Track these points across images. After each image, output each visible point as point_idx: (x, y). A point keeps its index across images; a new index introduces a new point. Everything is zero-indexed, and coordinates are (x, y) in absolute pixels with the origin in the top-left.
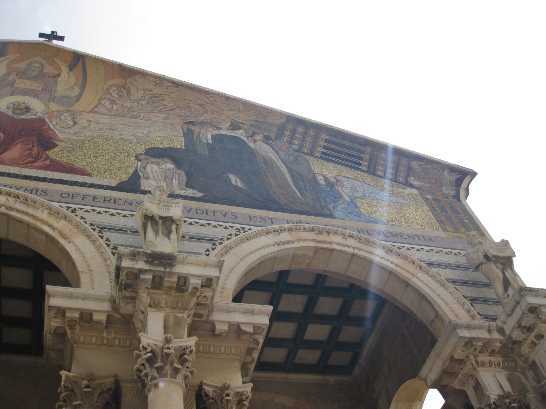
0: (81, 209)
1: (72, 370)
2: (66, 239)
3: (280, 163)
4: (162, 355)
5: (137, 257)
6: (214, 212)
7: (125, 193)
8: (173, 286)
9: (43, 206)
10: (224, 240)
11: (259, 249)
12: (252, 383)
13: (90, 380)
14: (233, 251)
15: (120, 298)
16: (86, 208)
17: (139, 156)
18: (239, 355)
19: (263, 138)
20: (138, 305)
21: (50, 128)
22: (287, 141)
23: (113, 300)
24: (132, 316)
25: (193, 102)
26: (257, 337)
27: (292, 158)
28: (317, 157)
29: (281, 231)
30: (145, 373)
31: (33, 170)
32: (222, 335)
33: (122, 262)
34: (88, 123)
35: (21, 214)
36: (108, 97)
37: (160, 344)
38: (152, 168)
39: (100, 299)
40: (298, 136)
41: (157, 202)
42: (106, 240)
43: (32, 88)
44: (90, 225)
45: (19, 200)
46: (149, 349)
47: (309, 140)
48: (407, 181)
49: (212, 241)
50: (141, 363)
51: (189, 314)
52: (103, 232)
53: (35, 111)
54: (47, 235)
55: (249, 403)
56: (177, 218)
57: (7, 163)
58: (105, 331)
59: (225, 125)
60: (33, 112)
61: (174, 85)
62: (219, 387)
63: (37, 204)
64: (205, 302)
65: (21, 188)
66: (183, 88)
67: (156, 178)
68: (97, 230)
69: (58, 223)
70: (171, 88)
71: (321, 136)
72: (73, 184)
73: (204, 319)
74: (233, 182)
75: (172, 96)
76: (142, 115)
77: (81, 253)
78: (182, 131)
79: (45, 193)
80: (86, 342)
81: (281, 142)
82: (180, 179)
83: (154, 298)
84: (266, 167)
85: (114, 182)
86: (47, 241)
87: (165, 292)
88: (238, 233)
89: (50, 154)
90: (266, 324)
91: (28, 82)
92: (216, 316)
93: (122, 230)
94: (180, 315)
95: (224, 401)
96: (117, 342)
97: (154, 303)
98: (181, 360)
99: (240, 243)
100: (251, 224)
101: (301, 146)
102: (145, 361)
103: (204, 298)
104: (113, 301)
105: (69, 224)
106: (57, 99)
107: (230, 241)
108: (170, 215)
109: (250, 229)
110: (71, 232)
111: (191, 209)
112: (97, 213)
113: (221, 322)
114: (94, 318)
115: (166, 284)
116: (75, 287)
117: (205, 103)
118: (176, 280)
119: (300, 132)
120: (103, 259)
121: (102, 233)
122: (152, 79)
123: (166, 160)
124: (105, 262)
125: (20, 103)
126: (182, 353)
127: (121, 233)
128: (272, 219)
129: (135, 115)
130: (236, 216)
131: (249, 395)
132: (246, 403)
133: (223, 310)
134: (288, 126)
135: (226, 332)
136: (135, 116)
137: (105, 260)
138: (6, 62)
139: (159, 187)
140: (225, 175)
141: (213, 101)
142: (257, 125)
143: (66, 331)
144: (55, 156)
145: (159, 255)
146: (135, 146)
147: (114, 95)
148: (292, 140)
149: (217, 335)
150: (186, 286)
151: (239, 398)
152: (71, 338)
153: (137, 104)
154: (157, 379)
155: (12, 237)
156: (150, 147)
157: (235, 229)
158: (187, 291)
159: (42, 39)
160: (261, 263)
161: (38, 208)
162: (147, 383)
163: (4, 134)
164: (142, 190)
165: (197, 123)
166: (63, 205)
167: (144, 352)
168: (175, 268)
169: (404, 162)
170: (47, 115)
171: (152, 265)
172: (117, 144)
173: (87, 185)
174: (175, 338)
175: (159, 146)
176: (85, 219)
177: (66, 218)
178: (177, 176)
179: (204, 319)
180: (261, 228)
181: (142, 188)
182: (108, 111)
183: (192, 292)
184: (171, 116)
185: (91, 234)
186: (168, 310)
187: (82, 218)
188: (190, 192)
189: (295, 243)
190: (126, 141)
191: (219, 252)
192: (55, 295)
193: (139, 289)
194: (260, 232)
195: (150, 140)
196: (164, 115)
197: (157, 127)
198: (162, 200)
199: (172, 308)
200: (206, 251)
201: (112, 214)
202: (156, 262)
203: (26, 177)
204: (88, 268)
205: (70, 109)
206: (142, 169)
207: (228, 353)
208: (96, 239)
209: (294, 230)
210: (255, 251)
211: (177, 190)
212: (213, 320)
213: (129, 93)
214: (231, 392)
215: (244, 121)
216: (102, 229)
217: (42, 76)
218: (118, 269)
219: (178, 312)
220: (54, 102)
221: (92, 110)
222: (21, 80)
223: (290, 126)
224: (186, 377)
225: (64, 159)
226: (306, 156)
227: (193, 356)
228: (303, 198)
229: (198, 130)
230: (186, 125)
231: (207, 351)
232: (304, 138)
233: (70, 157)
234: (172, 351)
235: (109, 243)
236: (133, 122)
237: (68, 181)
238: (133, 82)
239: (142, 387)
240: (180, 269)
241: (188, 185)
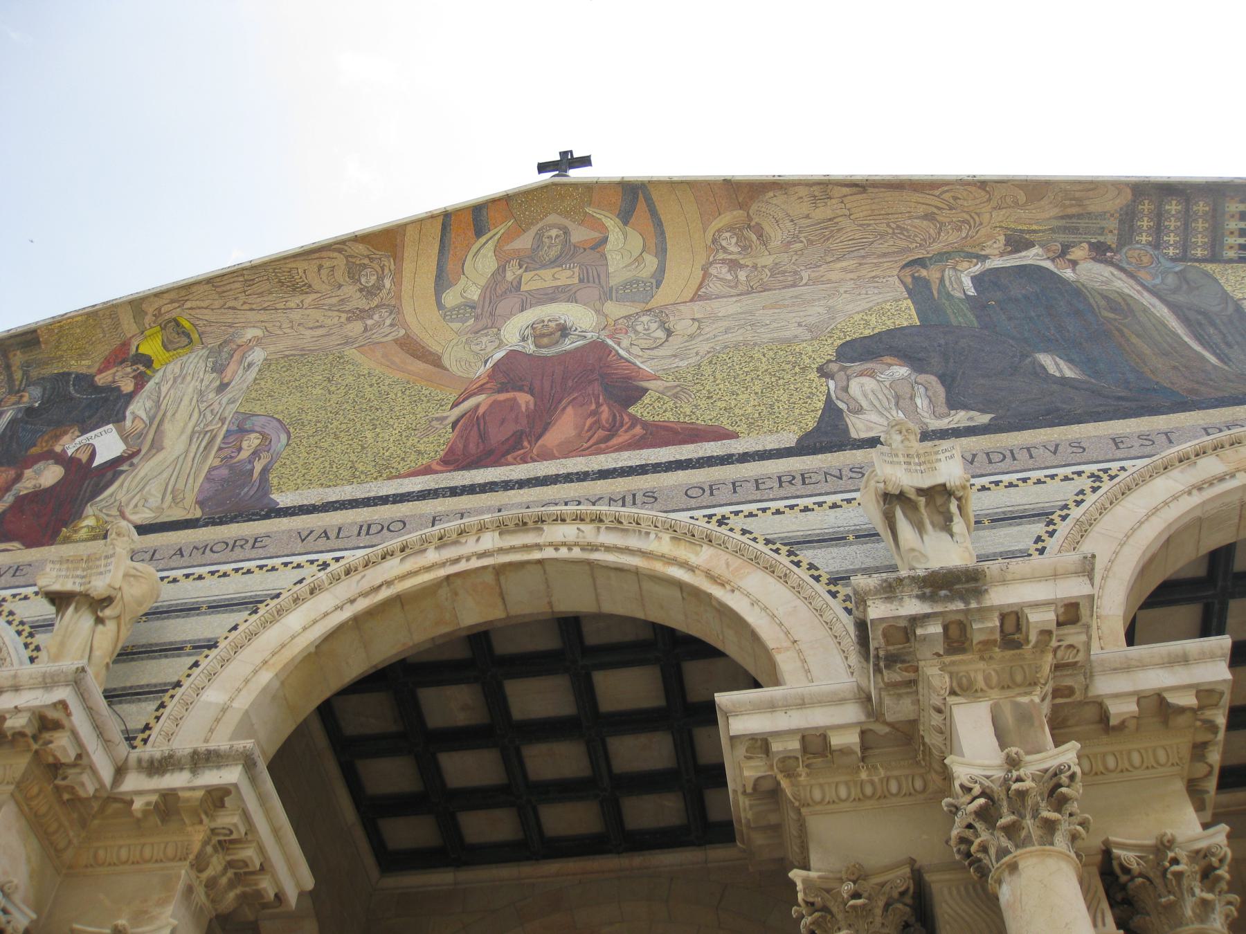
0: (736, 513)
1: (812, 865)
2: (723, 585)
3: (1147, 299)
4: (1008, 797)
5: (897, 591)
6: (1028, 449)
7: (820, 456)
8: (993, 637)
9: (656, 526)
10: (1069, 509)
11: (1156, 510)
12: (1227, 824)
13: (857, 879)
14: (1098, 528)
15: (880, 689)
16: (747, 508)
17: (825, 367)
18: (1177, 764)
19: (1090, 250)
20: (923, 696)
21: (622, 358)
22: (1149, 243)
23: (863, 695)
24: (914, 723)
25: (907, 215)
26: (1207, 714)
27: (1171, 280)
28: (1230, 261)
29: (1197, 455)
30: (980, 844)
31: (614, 455)
32: (1126, 727)
33: (869, 609)
34: (696, 324)
35: (616, 554)
36: (721, 258)
37: (999, 774)
38: (862, 386)
39: (836, 700)
40: (1173, 224)
41: (902, 459)
42: (809, 569)
43: (559, 283)
44: (766, 544)
45: (603, 527)
46: (977, 790)
47: (1200, 225)
49: (1044, 515)
50: (965, 823)
51: (1043, 693)
52: (798, 552)
53: (579, 329)
54: (680, 585)
55: (1229, 872)
56: (958, 483)
57: (557, 454)
58: (863, 767)
59: (995, 246)
60: (577, 333)
61: (855, 190)
62: (1151, 846)
63: (643, 525)
64: (1073, 658)
65: (600, 498)
66: (877, 190)
67: (878, 406)
68: (784, 549)
69: (697, 554)
70: (849, 197)
71: (1227, 209)
72: (703, 464)
73: (1078, 696)
74: (1052, 370)
75: (858, 215)
76: (805, 275)
77: (765, 609)
78: (901, 286)
79: (651, 497)
80: (827, 800)
81: (1135, 249)
82: (930, 393)
83: (957, 673)
84: (1117, 317)
85: (789, 439)
86: (683, 598)
87: (977, 656)
88: (1097, 484)
89: (637, 411)
90: (1225, 681)
91: (547, 273)
92: (1104, 686)
93: (836, 539)
94: (1024, 700)
95: (1169, 876)
96: (894, 787)
97: (960, 685)
98: (1053, 800)
99: (1107, 505)
100: (1122, 456)
101: (1185, 246)
102: (973, 816)
103: (1069, 651)
104: (865, 699)
105: (720, 552)
106: (617, 292)
107: (1084, 506)
108: (940, 481)
109: (1123, 469)
110: (731, 569)
111: (974, 456)
112: (773, 514)
113: (1116, 696)
114: (832, 743)
115: (977, 638)
116: (768, 686)
117: (936, 211)
118: (998, 624)
119: (1173, 212)
120: (814, 611)
121: (796, 555)
122: (803, 191)
123: (888, 359)
124: (821, 615)
125: (543, 321)
126: (1052, 783)
127: (836, 545)
128: (1166, 434)
129: (790, 279)
130: (1081, 447)
131: (1225, 855)
132: (1223, 872)
133: (1115, 669)
134: (1140, 207)
135: (1135, 717)
136: (791, 283)
137: (820, 612)
138: (491, 245)
139: (896, 425)
140: (1029, 359)
141: (952, 201)
142: (1068, 225)
143: (778, 783)
144: (648, 413)
145: (945, 575)
146: (810, 349)
147: (731, 249)
149: (1115, 728)
150: (1021, 633)
151: (1204, 863)
152: (794, 798)
153: (786, 255)
154: (1011, 853)
155: (608, 608)
156: (844, 341)
157: (1089, 477)
158: (1028, 641)
159: (547, 176)
160: (1169, 542)
161: (648, 534)
162: (990, 866)
163: (532, 395)
164: (855, 439)
165: (930, 259)
166: (696, 513)
167: (968, 798)
168: (987, 596)
170: (606, 332)
171: (937, 602)
172: (771, 353)
173: (734, 458)
174: (1028, 753)
175: (862, 333)
176: (751, 533)
177: (710, 541)
178: (922, 390)
179: (1078, 696)
180: (1146, 461)
181: (854, 435)
182: (729, 287)
183: (1037, 642)
184: (868, 260)
185: (774, 562)
186: (995, 694)
187: (744, 532)
188: (961, 418)
189: (1238, 475)
190: (789, 341)
191: (1066, 538)
192: (737, 711)
193: (918, 661)
194: (1148, 470)
195: (839, 326)
196: (852, 262)
197: (845, 292)
198: (912, 452)
199: (1003, 688)
200: (1036, 542)
201: (806, 509)
202: (943, 593)
203: (604, 474)
204: (789, 638)
205: (649, 306)
206: (839, 392)
207: (1150, 766)
208: (788, 571)
209: (1227, 446)
210: (1148, 517)
211: (932, 421)
212: (1099, 696)
213: (761, 236)
214: (1182, 854)
215: (1035, 224)
216: (794, 545)
217: (572, 252)
218: (862, 627)
219: (1020, 695)
220: (612, 300)
221: (696, 293)
222: (532, 273)
224: (1074, 837)
225: (669, 416)
226: (1203, 265)
227: (1078, 785)
228: (1225, 363)
229: (938, 275)
230: (908, 270)
231: (1101, 768)
232: (1186, 225)
233: (681, 407)
234: (1028, 784)
235: (816, 573)
236: (790, 295)
237: (690, 460)
238: (763, 209)
239: (979, 875)
240: (999, 597)
241: (954, 404)
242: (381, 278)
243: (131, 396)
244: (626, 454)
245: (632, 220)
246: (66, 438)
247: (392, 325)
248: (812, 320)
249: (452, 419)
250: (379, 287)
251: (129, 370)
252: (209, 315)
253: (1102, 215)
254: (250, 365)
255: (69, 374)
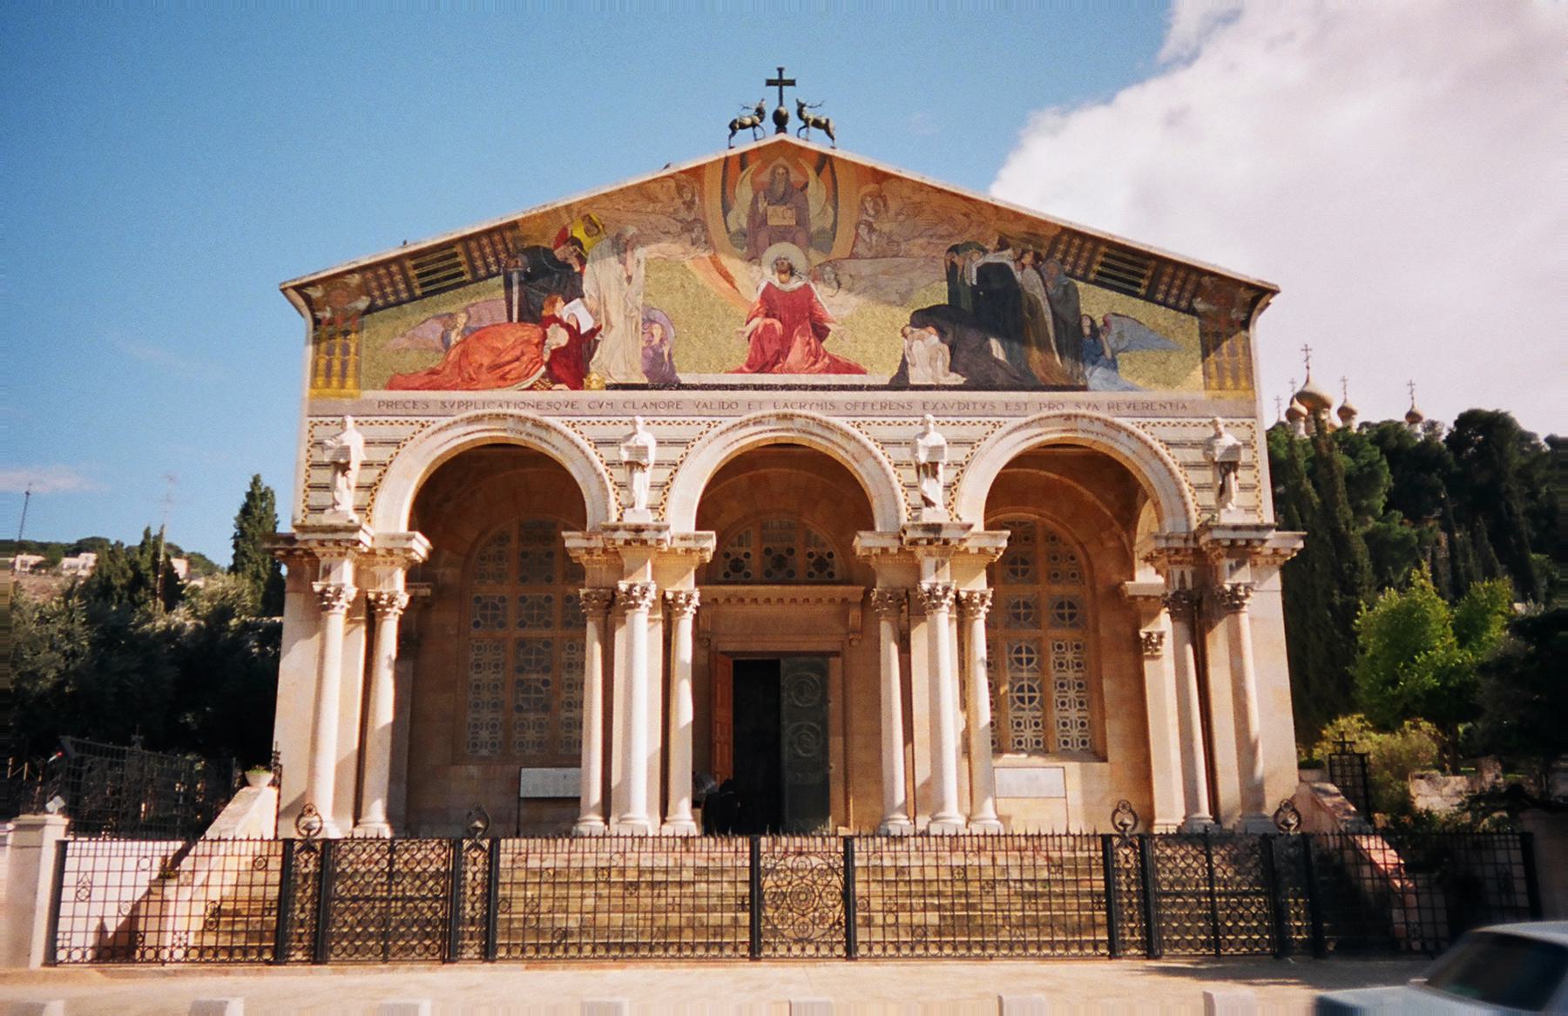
3: (1045, 306)
43: (785, 223)
47: (1085, 255)
48: (1190, 303)
74: (994, 353)
76: (903, 246)
91: (780, 209)
101: (1075, 266)
123: (931, 329)
138: (748, 177)
148: (1065, 257)
169: (1193, 277)
184: (934, 240)
203: (814, 388)
213: (885, 205)
223: (1065, 238)
240: (944, 535)
241: (952, 369)
242: (693, 195)
243: (581, 274)
244: (823, 375)
245: (822, 174)
246: (560, 304)
247: (706, 242)
248: (903, 290)
249: (747, 334)
250: (693, 202)
251: (571, 249)
252: (604, 213)
253: (1045, 237)
254: (639, 262)
255: (538, 247)
